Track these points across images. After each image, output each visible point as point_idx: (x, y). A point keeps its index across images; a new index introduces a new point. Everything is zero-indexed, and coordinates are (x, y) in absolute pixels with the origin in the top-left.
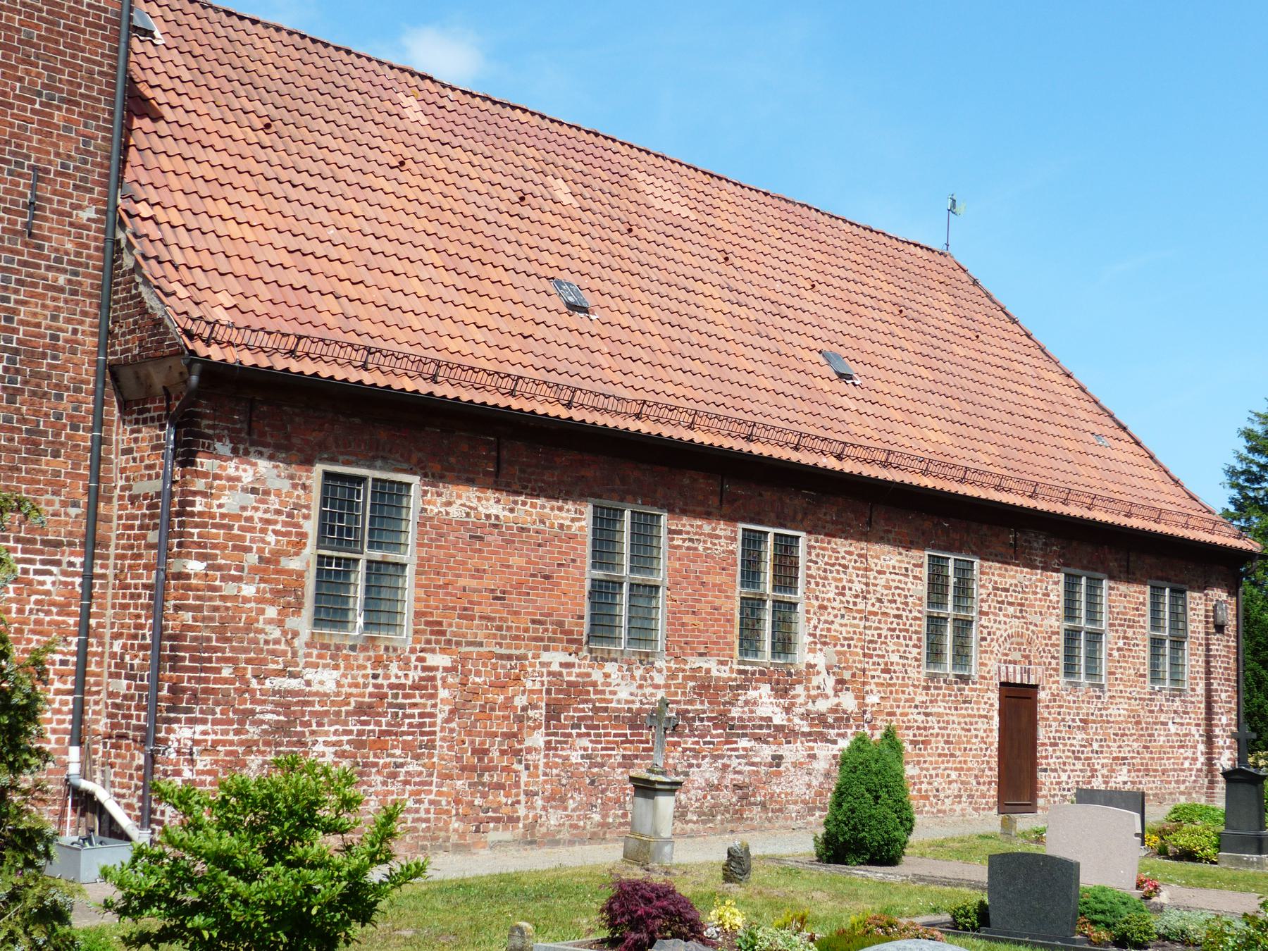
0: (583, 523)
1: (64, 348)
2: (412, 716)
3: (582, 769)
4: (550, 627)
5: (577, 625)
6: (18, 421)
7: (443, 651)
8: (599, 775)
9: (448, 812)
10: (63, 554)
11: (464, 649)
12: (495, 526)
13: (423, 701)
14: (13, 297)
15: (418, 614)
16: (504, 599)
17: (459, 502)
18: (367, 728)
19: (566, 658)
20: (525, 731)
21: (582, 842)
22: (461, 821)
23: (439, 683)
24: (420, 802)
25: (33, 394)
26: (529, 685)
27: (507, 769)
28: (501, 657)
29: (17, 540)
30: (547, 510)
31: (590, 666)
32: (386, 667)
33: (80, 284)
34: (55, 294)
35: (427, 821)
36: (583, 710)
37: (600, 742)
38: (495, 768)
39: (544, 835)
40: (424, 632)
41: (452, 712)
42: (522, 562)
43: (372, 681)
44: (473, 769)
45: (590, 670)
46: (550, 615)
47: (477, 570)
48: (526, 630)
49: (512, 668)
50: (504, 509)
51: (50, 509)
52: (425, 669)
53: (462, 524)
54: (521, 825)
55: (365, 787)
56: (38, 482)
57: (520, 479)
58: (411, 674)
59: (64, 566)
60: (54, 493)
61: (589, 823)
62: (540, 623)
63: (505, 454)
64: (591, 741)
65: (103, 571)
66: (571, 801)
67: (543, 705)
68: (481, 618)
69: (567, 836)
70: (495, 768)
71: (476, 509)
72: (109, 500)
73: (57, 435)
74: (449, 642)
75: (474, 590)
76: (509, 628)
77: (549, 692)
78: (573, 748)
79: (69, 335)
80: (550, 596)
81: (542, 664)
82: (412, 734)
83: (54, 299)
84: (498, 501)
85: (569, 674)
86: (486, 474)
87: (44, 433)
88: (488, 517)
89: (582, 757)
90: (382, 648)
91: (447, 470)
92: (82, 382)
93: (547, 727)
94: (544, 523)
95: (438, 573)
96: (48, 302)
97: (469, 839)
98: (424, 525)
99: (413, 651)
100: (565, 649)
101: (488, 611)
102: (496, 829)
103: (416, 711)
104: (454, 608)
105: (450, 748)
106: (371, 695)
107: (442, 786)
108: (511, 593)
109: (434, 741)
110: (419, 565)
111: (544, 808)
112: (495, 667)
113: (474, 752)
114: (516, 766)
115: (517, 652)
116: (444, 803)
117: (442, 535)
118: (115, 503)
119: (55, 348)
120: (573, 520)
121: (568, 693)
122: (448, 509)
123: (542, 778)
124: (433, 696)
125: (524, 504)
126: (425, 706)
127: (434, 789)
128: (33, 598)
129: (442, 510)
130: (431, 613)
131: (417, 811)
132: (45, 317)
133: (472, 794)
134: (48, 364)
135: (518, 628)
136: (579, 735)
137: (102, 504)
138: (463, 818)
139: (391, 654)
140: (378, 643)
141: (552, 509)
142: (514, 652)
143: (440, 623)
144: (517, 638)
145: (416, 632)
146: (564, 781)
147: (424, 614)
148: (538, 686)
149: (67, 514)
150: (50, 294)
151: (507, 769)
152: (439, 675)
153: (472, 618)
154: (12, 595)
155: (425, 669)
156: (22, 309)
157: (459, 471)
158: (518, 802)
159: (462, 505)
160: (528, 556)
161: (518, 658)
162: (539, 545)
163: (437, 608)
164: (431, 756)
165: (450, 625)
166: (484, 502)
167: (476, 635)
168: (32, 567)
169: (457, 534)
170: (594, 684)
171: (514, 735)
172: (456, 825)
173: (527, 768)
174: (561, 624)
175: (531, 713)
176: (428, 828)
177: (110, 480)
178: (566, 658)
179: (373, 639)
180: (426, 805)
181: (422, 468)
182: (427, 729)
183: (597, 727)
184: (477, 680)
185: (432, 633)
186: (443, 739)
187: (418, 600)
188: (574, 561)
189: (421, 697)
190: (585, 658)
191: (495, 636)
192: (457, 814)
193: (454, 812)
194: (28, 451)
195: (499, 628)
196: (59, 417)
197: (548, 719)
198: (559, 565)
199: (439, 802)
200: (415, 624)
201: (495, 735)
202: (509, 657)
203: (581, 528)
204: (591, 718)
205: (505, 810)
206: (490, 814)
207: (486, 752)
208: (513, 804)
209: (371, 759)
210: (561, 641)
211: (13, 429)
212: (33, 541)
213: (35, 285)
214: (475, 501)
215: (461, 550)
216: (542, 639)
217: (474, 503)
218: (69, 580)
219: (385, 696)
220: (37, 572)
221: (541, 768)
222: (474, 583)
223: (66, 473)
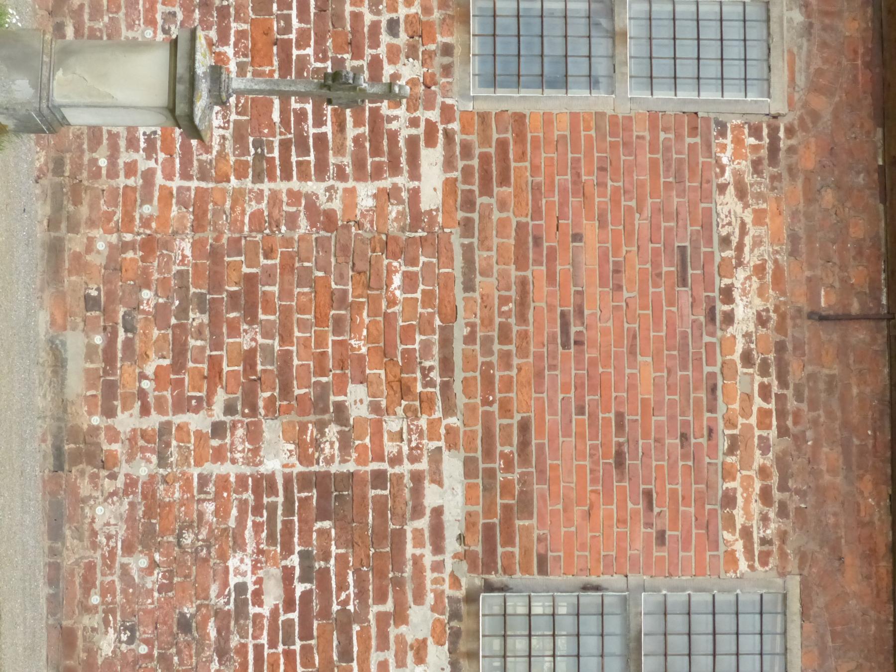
0: (743, 565)
2: (319, 121)
3: (214, 590)
4: (515, 476)
5: (526, 552)
7: (450, 186)
8: (201, 643)
9: (128, 218)
11: (457, 242)
12: (711, 314)
13: (350, 144)
15: (519, 118)
16: (566, 345)
17: (749, 218)
18: (294, 13)
19: (452, 529)
20: (294, 417)
21: (55, 603)
22: (110, 258)
23: (386, 183)
24: (150, 150)
26: (393, 424)
27: (214, 374)
28: (446, 342)
30: (758, 459)
31: (439, 595)
32: (412, 52)
35: (113, 173)
36: (342, 586)
37: (273, 644)
38: (217, 345)
39: (73, 490)
40: (485, 140)
41: (329, 220)
42: (646, 392)
43: (384, 18)
44: (216, 285)
45: (430, 598)
46: (541, 472)
47: (617, 271)
48: (505, 410)
49: (426, 372)
50: (747, 335)
52: (412, 142)
53: (707, 226)
54: (96, 420)
55: (180, 16)
57: (811, 377)
58: (401, 111)
61: (95, 621)
62: (524, 445)
63: (860, 335)
64: (275, 612)
66: (144, 562)
67: (351, 467)
68: (523, 283)
69: (68, 560)
70: (217, 345)
71: (740, 263)
74: (469, 203)
75: (575, 264)
76: (506, 357)
77: (379, 478)
78: (260, 558)
80: (581, 468)
81: (436, 456)
82: (285, 121)
84: (762, 321)
85: (419, 542)
86: (813, 284)
88: (727, 295)
89: (241, 588)
90: (447, 40)
91: (807, 180)
93: (305, 481)
94: (731, 451)
95: (602, 169)
97: (70, 280)
98: (693, 131)
99: (447, 113)
100: (470, 520)
101: (539, 301)
102: (90, 352)
103: (328, 129)
104: (537, 213)
105: (256, 217)
106: (357, 17)
107: (183, 203)
108: (579, 362)
109: (272, 178)
110: (614, 119)
111: (131, 483)
112: (426, 326)
113: (250, 281)
114: (220, 397)
115: (458, 387)
116: (147, 209)
117: (680, 180)
120: (746, 533)
121: (380, 535)
122: (731, 190)
123: (195, 472)
124: (359, 165)
125: (765, 393)
126: (340, 150)
127: (176, 183)
129: (728, 176)
130: (522, 157)
131: (132, 143)
133: (164, 282)
135: (507, 384)
136: (287, 576)
138: (114, 266)
139: (439, 60)
140: (457, 28)
141: (763, 472)
142: (459, 374)
143: (504, 180)
144: (488, 381)
145: (484, 117)
146: (188, 539)
147: (520, 137)
148: (390, 447)
151: (214, 374)
152: (402, 181)
153: (521, 262)
155: (412, 142)
157: (808, 216)
158: (145, 411)
159: (743, 225)
160: (659, 403)
161: (446, 387)
162: (684, 437)
163: (535, 169)
164: (240, 176)
165: (503, 205)
166: (755, 282)
167: (485, 273)
169: (684, 213)
170: (400, 616)
171: (286, 390)
172: (101, 246)
173: (218, 429)
174: (525, 506)
175: (332, 431)
176: (96, 174)
178: (452, 529)
179: (464, 18)
180: (144, 165)
181: (801, 120)
182: (294, 159)
183: (306, 634)
184: (397, 280)
185: (485, 159)
186: (275, 198)
187: (548, 119)
188: (661, 537)
189: (357, 140)
190: (455, 582)
191: (487, 322)
192: (125, 246)
193: (128, 237)
195: (505, 336)
197: (321, 481)
198: (648, 494)
199: (147, 199)
200: (500, 115)
201: (286, 337)
202: (447, 365)
203: (731, 559)
204: (325, 613)
205: (125, 372)
206: (122, 335)
207: (251, 317)
208: (142, 394)
209: (234, 26)
210: (489, 510)
214: (755, 261)
215: (654, 227)
216: (488, 454)
217: (750, 258)
219: (358, 54)
221: (216, 469)
222: (589, 260)
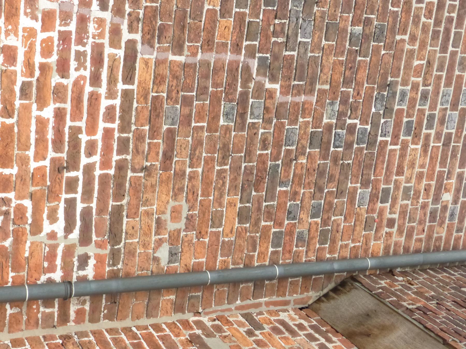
1: (373, 211)
6: (288, 151)
10: (99, 245)
14: (433, 132)
25: (321, 174)
29: (121, 167)
33: (441, 223)
34: (433, 188)
51: (167, 217)
56: (206, 193)
59: (80, 251)
60: (189, 219)
65: (72, 315)
72: (179, 308)
73: (269, 215)
79: (388, 215)
83: (427, 190)
87: (271, 195)
92: (333, 242)
96: (424, 182)
118: (175, 317)
119: (373, 198)
128: (28, 203)
132: (408, 181)
134: (355, 189)
137: (173, 297)
149: (159, 243)
150: (433, 183)
154: (33, 165)
156: (419, 147)
168: (78, 196)
177: (207, 304)
194: (248, 171)
196: (291, 214)
211: (278, 145)
212: (119, 196)
213: (443, 164)
218: (59, 261)
220: (71, 204)
223: (217, 234)
